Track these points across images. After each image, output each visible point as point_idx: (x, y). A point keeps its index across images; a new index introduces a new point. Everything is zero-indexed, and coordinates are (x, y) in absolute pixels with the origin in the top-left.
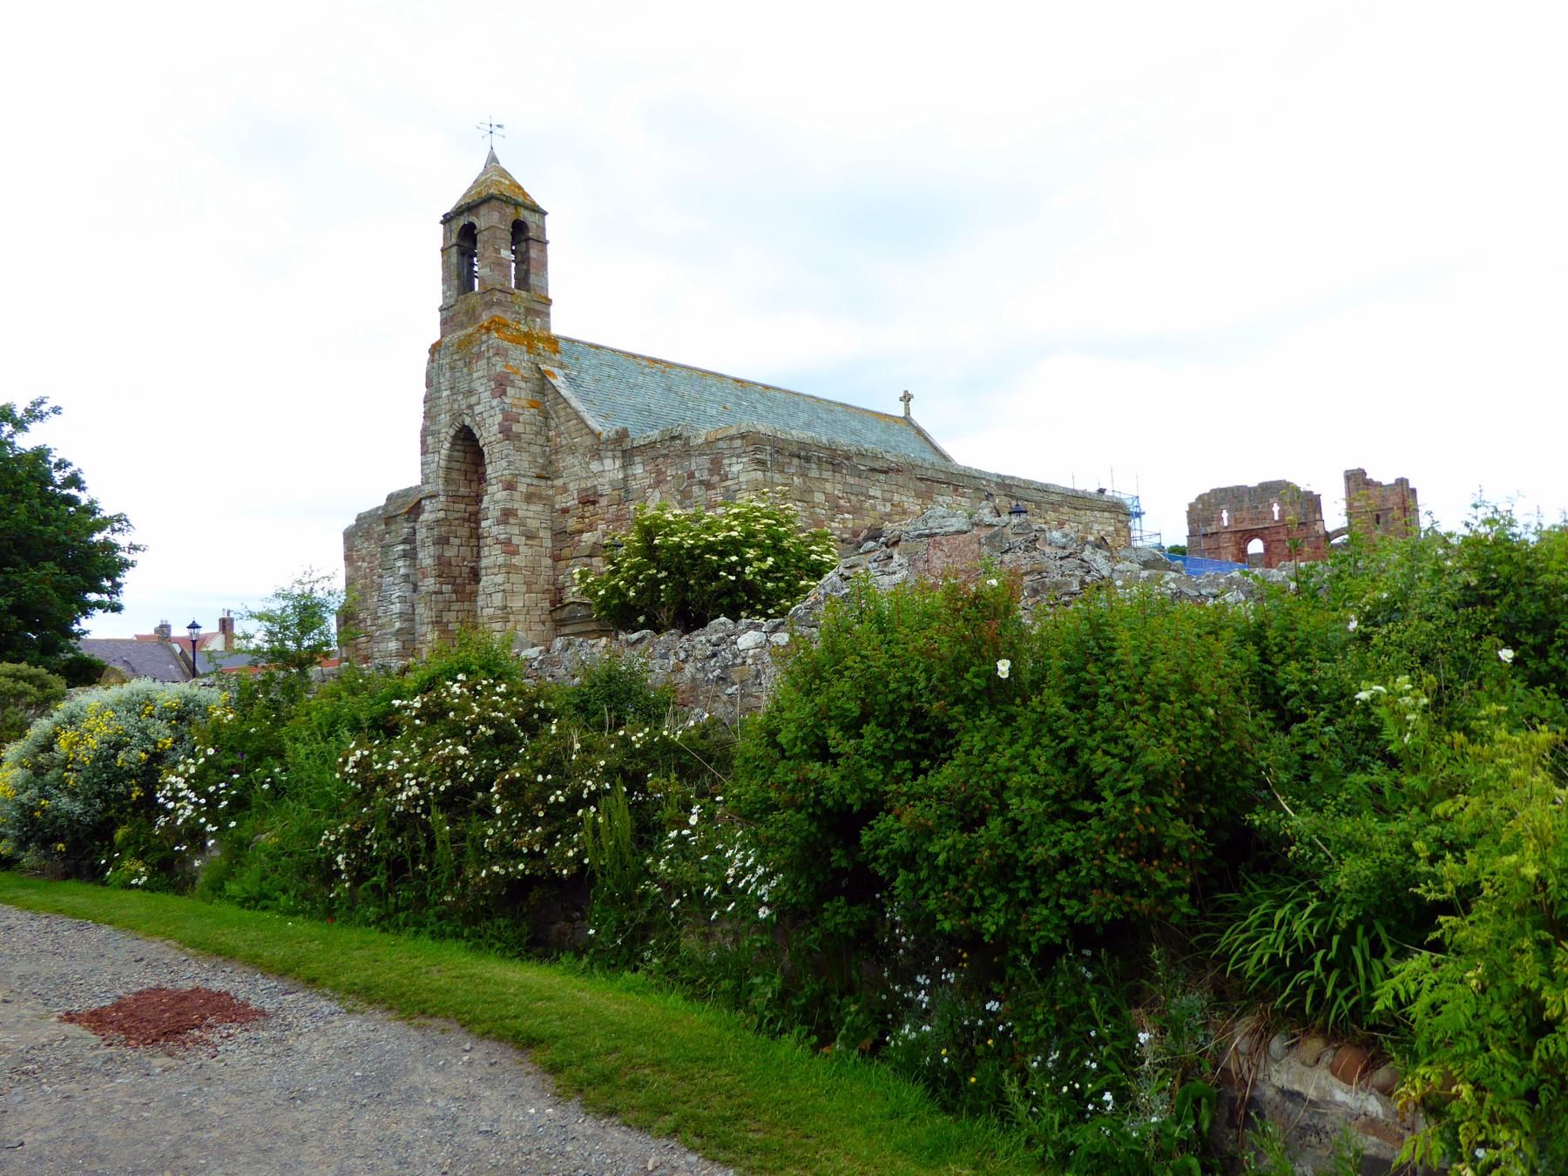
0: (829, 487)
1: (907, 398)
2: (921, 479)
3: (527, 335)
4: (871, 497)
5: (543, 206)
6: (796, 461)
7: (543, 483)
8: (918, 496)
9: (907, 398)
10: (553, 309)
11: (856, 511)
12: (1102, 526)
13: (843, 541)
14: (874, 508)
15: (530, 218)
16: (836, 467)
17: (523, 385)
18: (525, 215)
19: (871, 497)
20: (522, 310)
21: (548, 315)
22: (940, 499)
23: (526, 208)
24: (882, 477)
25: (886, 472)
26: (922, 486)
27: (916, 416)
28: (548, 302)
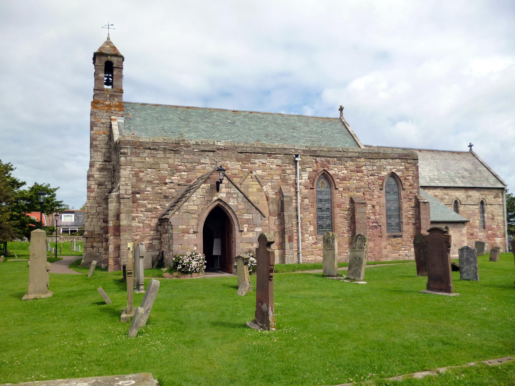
0: (171, 161)
1: (341, 109)
2: (241, 153)
3: (109, 106)
4: (202, 163)
5: (122, 52)
6: (148, 151)
7: (107, 163)
8: (238, 160)
9: (341, 109)
10: (124, 95)
11: (188, 170)
12: (398, 168)
13: (179, 185)
14: (204, 168)
15: (114, 60)
16: (176, 152)
17: (102, 125)
18: (109, 58)
19: (202, 163)
20: (108, 96)
21: (122, 96)
22: (257, 161)
23: (112, 55)
24: (212, 154)
25: (214, 151)
26: (243, 156)
27: (346, 118)
28: (121, 91)
